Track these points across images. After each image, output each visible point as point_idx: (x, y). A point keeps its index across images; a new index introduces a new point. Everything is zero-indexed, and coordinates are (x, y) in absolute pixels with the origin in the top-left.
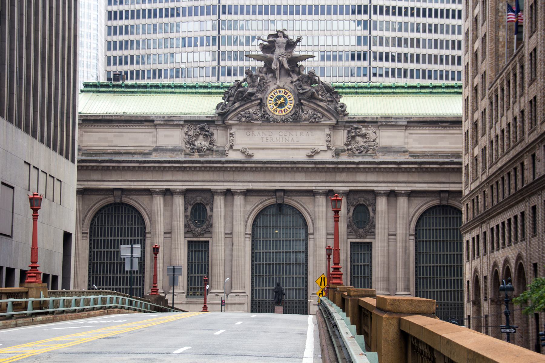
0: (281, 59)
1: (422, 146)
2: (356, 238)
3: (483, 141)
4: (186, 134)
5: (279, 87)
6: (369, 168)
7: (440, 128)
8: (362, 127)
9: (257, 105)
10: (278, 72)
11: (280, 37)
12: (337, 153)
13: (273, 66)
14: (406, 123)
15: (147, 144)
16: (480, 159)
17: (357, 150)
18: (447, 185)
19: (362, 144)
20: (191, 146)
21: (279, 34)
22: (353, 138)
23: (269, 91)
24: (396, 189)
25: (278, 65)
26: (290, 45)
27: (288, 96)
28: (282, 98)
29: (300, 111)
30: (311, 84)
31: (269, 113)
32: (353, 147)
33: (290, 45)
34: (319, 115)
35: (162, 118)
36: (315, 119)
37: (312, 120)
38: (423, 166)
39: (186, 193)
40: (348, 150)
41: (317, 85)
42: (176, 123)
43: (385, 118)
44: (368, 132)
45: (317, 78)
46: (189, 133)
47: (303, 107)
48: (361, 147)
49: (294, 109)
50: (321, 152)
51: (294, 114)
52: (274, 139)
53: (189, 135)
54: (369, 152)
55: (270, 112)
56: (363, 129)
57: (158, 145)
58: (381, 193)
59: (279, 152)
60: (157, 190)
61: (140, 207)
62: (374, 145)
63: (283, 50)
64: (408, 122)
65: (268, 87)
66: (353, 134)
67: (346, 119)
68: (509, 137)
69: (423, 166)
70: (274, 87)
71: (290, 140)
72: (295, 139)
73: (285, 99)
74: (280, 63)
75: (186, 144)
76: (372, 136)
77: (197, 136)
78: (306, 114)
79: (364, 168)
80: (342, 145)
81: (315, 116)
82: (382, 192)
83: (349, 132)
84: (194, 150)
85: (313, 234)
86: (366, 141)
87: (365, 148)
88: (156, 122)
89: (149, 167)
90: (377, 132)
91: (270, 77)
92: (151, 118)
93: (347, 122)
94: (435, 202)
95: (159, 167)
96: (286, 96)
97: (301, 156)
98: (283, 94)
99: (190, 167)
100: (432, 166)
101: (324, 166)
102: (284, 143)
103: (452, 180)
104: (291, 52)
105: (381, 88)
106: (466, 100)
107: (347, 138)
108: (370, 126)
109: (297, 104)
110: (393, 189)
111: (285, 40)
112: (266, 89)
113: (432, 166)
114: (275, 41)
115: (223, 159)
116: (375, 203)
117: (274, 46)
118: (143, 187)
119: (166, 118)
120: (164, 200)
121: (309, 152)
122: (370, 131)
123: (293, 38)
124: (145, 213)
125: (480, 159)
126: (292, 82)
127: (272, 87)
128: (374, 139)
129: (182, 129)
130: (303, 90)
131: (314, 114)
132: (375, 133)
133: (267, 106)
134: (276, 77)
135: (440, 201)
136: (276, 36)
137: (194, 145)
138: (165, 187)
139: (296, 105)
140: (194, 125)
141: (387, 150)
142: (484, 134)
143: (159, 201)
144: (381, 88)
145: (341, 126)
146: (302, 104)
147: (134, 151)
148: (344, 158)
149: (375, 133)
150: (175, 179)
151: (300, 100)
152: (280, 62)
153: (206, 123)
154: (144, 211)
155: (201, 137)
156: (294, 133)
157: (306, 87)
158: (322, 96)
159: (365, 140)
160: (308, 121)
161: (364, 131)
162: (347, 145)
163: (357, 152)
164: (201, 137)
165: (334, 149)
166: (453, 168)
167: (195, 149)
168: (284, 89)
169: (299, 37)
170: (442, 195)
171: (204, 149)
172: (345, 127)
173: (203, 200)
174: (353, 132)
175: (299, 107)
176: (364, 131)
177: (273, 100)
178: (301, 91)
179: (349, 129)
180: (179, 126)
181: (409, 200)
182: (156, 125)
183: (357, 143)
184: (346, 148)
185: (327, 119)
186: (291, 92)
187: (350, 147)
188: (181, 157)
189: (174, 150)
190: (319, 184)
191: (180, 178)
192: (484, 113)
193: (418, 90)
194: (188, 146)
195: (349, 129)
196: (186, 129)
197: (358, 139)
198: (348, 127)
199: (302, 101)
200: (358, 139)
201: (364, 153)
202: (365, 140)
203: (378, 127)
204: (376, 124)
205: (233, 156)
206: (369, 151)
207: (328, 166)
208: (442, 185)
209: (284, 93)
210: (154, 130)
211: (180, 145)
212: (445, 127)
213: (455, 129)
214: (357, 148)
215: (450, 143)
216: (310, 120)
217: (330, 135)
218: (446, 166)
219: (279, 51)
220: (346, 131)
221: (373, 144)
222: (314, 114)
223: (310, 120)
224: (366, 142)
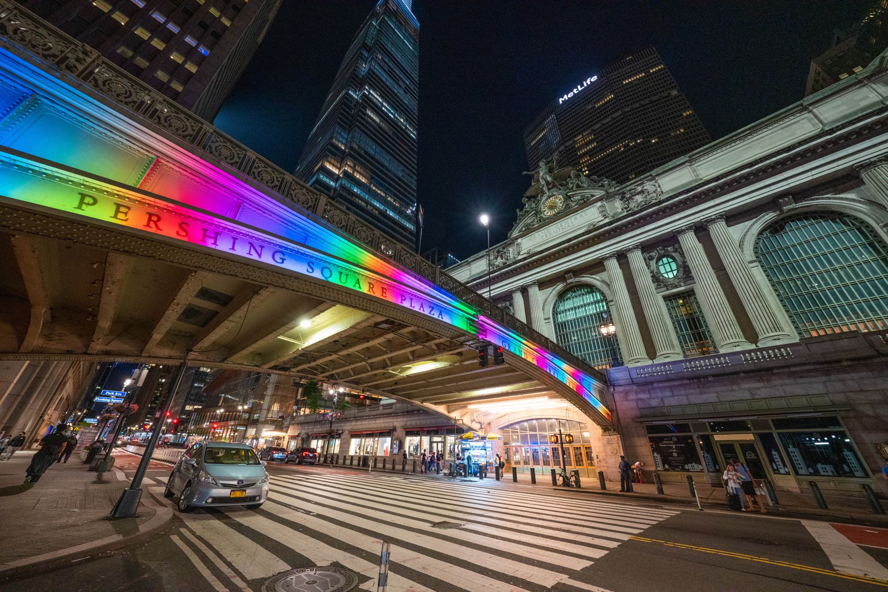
2: (668, 290)
44: (645, 188)
48: (641, 202)
52: (553, 233)
71: (566, 227)
72: (570, 224)
77: (496, 258)
85: (612, 301)
102: (561, 232)
146: (569, 197)
156: (569, 220)
164: (499, 258)
176: (639, 189)
190: (604, 250)
199: (569, 194)
212: (745, 136)
215: (762, 149)
217: (603, 206)
221: (655, 195)
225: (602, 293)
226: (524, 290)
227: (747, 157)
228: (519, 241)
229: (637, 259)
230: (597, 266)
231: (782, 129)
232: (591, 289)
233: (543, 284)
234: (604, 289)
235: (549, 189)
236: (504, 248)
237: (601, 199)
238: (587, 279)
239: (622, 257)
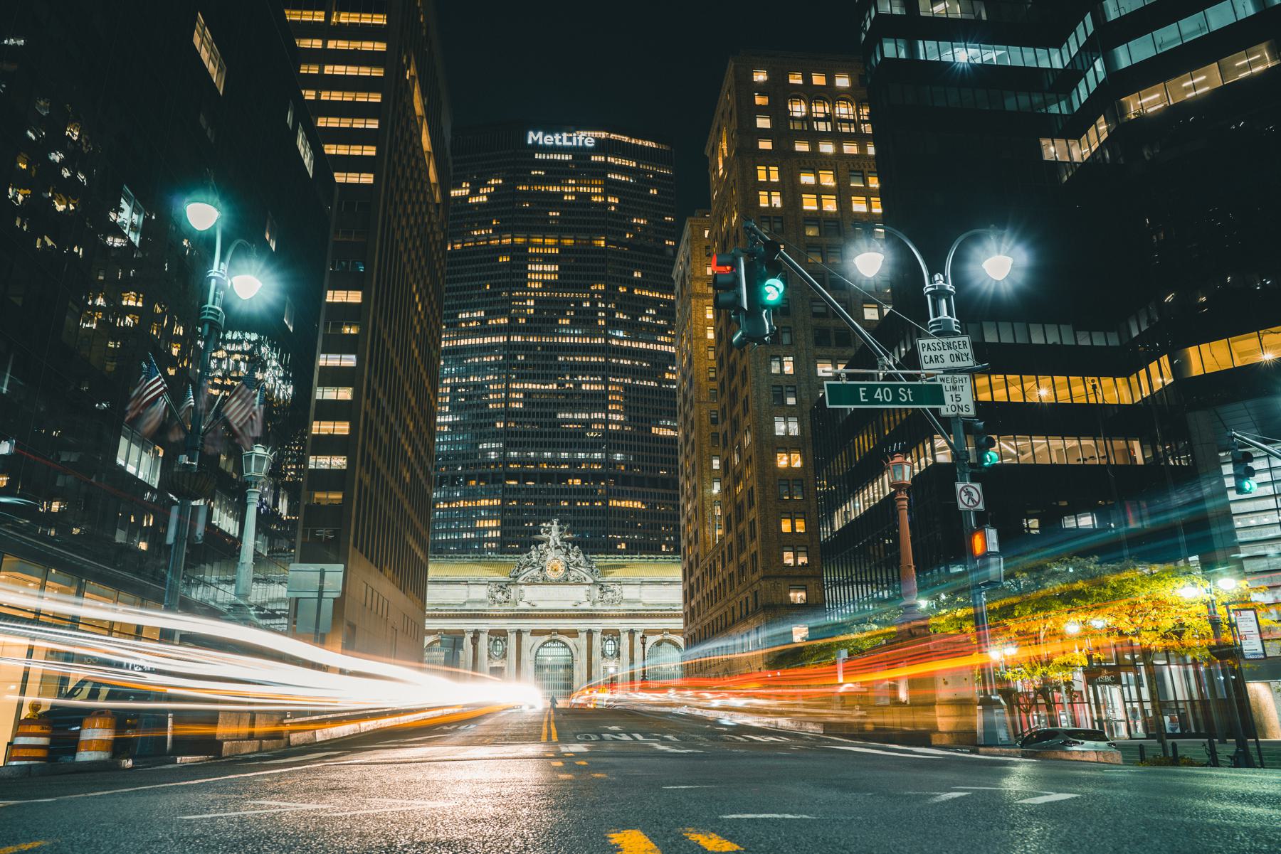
3: (698, 597)
12: (594, 603)
16: (696, 609)
59: (554, 602)
68: (716, 595)
76: (618, 592)
77: (497, 592)
97: (568, 606)
106: (684, 571)
115: (515, 608)
121: (573, 603)
122: (617, 588)
125: (696, 609)
141: (628, 601)
142: (698, 590)
148: (599, 606)
155: (500, 593)
164: (500, 593)
176: (612, 588)
188: (485, 607)
189: (482, 602)
192: (698, 579)
196: (490, 587)
200: (609, 593)
205: (522, 605)
225: (571, 651)
226: (519, 633)
228: (523, 587)
229: (597, 638)
230: (573, 634)
232: (566, 646)
233: (534, 633)
234: (574, 651)
235: (556, 548)
236: (506, 585)
237: (589, 584)
238: (564, 638)
239: (590, 633)
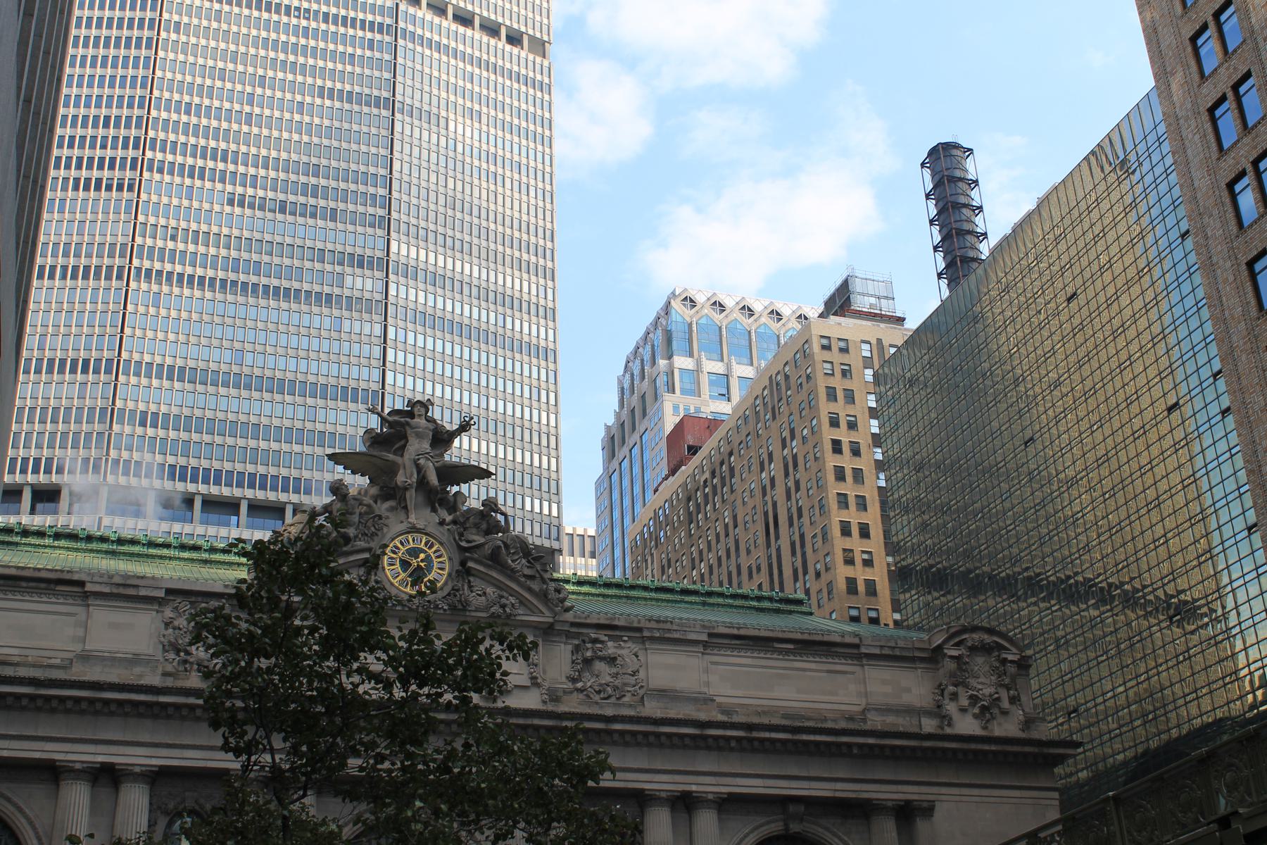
0: (422, 462)
1: (740, 693)
4: (167, 625)
5: (414, 529)
6: (634, 734)
7: (775, 656)
8: (606, 638)
9: (360, 566)
10: (411, 495)
11: (420, 415)
13: (400, 478)
14: (704, 637)
15: (58, 646)
17: (599, 692)
18: (805, 784)
19: (609, 679)
20: (178, 654)
21: (416, 410)
22: (588, 662)
23: (389, 536)
24: (694, 788)
25: (415, 476)
26: (442, 439)
27: (435, 552)
28: (422, 556)
29: (466, 587)
30: (488, 532)
31: (387, 586)
32: (589, 684)
33: (442, 439)
34: (512, 600)
35: (105, 579)
36: (503, 606)
37: (495, 609)
38: (755, 734)
39: (157, 778)
40: (578, 690)
41: (500, 534)
42: (143, 592)
43: (658, 621)
44: (620, 652)
45: (500, 518)
46: (176, 623)
47: (472, 579)
49: (450, 582)
50: (515, 691)
51: (449, 594)
53: (174, 628)
54: (626, 699)
55: (392, 584)
56: (610, 644)
57: (87, 648)
58: (659, 798)
60: (78, 766)
61: (19, 815)
62: (633, 682)
63: (426, 446)
64: (710, 635)
65: (385, 530)
66: (589, 654)
67: (569, 616)
69: (755, 734)
70: (403, 527)
73: (428, 559)
74: (419, 472)
75: (165, 651)
76: (631, 663)
78: (480, 595)
79: (622, 733)
80: (564, 679)
81: (504, 601)
82: (663, 795)
83: (577, 649)
84: (187, 666)
86: (617, 674)
87: (615, 688)
88: (89, 587)
89: (62, 699)
90: (641, 654)
91: (388, 510)
92: (76, 577)
93: (573, 624)
94: (775, 827)
95: (92, 701)
96: (430, 552)
98: (422, 546)
99: (177, 707)
100: (774, 735)
101: (529, 721)
103: (813, 773)
104: (442, 455)
105: (600, 585)
107: (573, 662)
108: (626, 638)
109: (457, 571)
110: (687, 788)
111: (431, 426)
112: (379, 533)
113: (774, 735)
114: (408, 424)
116: (642, 823)
117: (404, 437)
118: (37, 755)
119: (117, 580)
120: (93, 799)
122: (626, 651)
123: (450, 422)
124: (31, 833)
126: (442, 523)
127: (395, 525)
128: (635, 669)
129: (158, 612)
130: (468, 542)
131: (502, 597)
132: (637, 656)
133: (383, 569)
134: (406, 508)
135: (786, 825)
136: (411, 414)
137: (188, 653)
138: (100, 759)
139: (454, 574)
140: (191, 603)
143: (77, 796)
144: (600, 585)
145: (560, 633)
147: (16, 659)
148: (572, 705)
149: (637, 656)
150: (128, 738)
151: (463, 563)
152: (419, 469)
153: (224, 601)
154: (28, 827)
157: (475, 538)
158: (513, 561)
159: (614, 670)
160: (487, 612)
161: (611, 648)
162: (574, 680)
163: (597, 698)
165: (546, 684)
166: (817, 744)
167: (192, 663)
168: (426, 534)
169: (467, 419)
170: (792, 808)
171: (216, 664)
172: (569, 635)
173: (202, 801)
174: (587, 649)
175: (464, 579)
176: (611, 648)
177: (403, 549)
178: (464, 544)
179: (576, 642)
180: (151, 603)
181: (720, 820)
182: (86, 595)
183: (597, 676)
184: (570, 685)
185: (529, 612)
186: (441, 544)
187: (579, 685)
189: (135, 660)
191: (146, 738)
193: (678, 597)
194: (172, 656)
195: (576, 642)
196: (168, 613)
197: (599, 666)
198: (573, 638)
199: (471, 564)
200: (599, 666)
201: (613, 700)
202: (614, 670)
203: (643, 643)
204: (638, 635)
206: (624, 696)
207: (537, 722)
208: (794, 784)
209: (426, 544)
210: (80, 610)
211: (151, 652)
212: (788, 652)
213: (805, 658)
214: (597, 688)
216: (493, 610)
218: (805, 737)
219: (417, 446)
220: (570, 647)
221: (632, 680)
222: (502, 597)
223: (493, 610)
224: (616, 675)
227: (775, 694)
231: (829, 672)
